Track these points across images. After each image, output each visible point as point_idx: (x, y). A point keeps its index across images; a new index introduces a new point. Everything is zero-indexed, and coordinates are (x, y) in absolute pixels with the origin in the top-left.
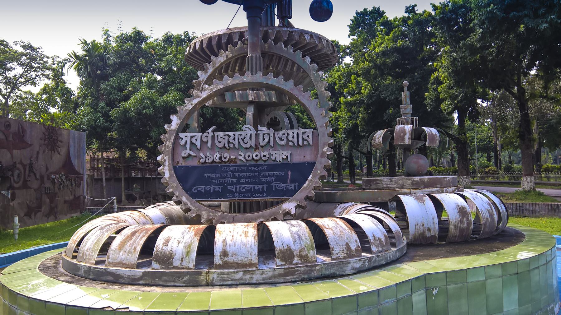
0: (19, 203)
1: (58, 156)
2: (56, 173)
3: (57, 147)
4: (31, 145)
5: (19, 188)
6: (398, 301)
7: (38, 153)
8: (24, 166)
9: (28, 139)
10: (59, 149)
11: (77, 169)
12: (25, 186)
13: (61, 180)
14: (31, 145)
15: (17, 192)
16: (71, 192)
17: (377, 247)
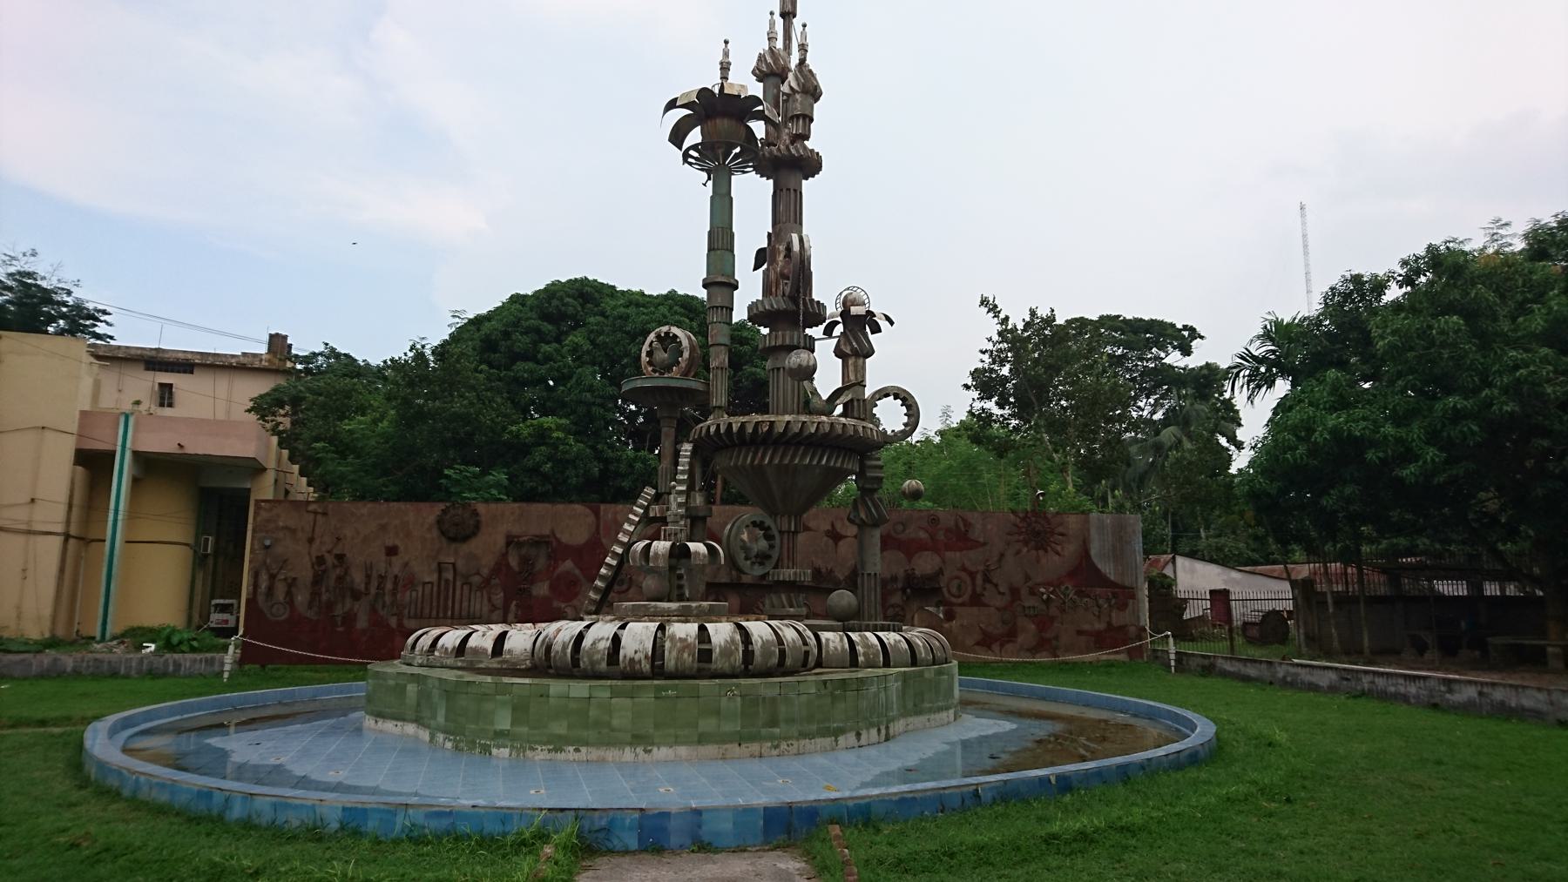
0: (962, 625)
1: (1056, 558)
2: (1047, 584)
3: (1053, 545)
4: (985, 544)
5: (962, 605)
6: (397, 684)
7: (1002, 555)
8: (972, 575)
9: (977, 533)
10: (1059, 548)
11: (1112, 578)
12: (976, 600)
13: (1064, 595)
14: (985, 544)
15: (958, 610)
16: (1099, 617)
17: (441, 653)
